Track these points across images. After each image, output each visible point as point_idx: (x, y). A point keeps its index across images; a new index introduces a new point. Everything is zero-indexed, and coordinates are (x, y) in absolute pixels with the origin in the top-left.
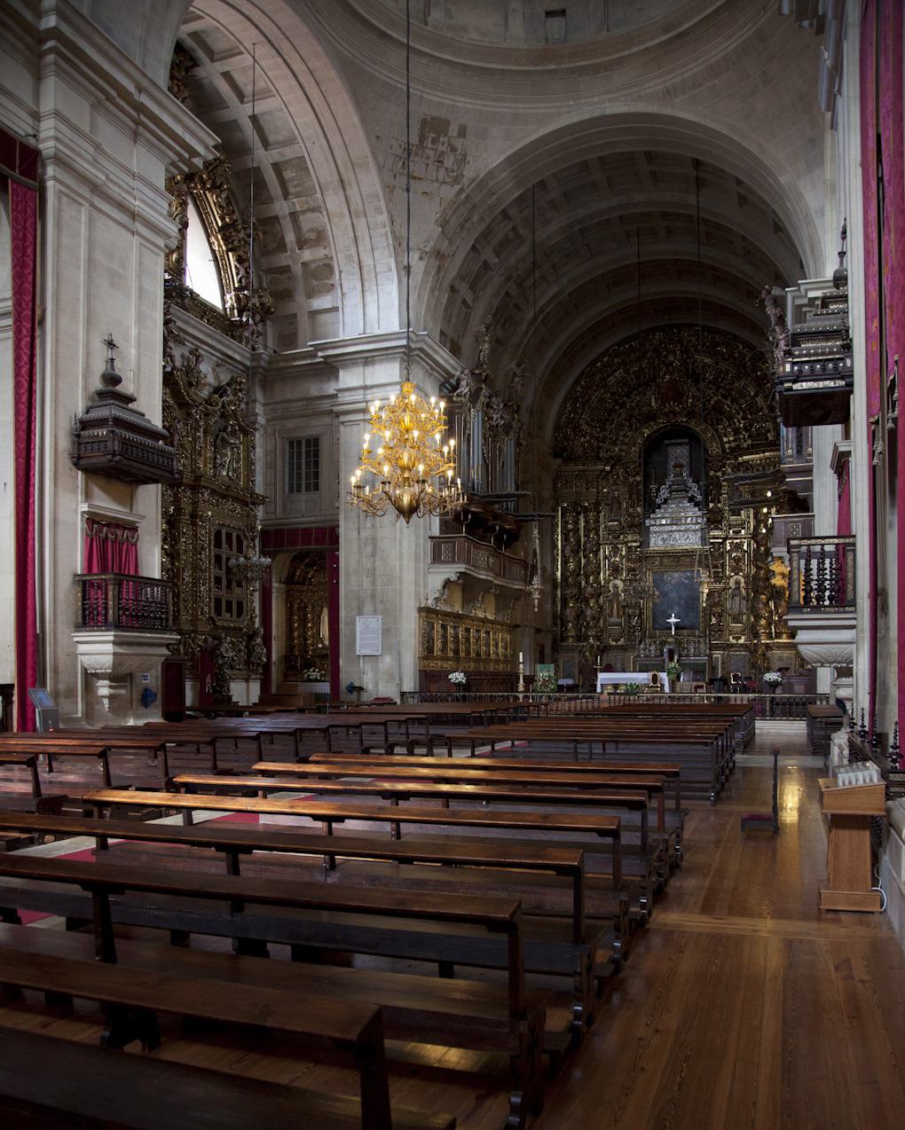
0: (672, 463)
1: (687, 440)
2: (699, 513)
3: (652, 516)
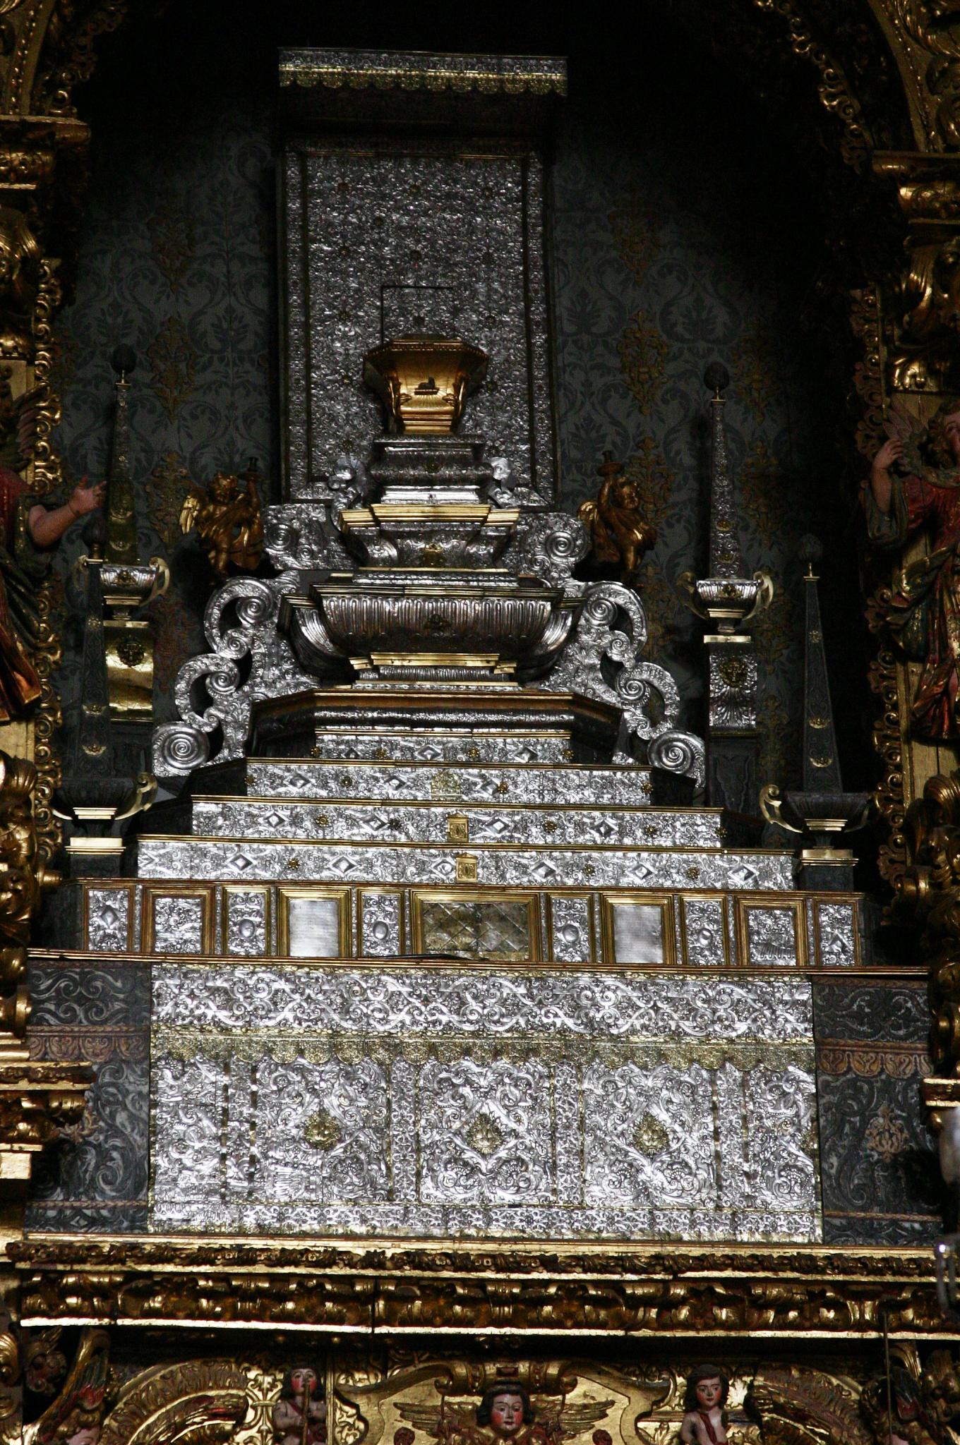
0: (346, 341)
1: (547, 74)
2: (739, 871)
3: (160, 857)
